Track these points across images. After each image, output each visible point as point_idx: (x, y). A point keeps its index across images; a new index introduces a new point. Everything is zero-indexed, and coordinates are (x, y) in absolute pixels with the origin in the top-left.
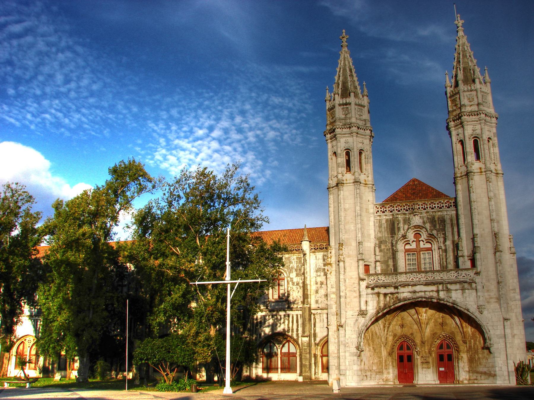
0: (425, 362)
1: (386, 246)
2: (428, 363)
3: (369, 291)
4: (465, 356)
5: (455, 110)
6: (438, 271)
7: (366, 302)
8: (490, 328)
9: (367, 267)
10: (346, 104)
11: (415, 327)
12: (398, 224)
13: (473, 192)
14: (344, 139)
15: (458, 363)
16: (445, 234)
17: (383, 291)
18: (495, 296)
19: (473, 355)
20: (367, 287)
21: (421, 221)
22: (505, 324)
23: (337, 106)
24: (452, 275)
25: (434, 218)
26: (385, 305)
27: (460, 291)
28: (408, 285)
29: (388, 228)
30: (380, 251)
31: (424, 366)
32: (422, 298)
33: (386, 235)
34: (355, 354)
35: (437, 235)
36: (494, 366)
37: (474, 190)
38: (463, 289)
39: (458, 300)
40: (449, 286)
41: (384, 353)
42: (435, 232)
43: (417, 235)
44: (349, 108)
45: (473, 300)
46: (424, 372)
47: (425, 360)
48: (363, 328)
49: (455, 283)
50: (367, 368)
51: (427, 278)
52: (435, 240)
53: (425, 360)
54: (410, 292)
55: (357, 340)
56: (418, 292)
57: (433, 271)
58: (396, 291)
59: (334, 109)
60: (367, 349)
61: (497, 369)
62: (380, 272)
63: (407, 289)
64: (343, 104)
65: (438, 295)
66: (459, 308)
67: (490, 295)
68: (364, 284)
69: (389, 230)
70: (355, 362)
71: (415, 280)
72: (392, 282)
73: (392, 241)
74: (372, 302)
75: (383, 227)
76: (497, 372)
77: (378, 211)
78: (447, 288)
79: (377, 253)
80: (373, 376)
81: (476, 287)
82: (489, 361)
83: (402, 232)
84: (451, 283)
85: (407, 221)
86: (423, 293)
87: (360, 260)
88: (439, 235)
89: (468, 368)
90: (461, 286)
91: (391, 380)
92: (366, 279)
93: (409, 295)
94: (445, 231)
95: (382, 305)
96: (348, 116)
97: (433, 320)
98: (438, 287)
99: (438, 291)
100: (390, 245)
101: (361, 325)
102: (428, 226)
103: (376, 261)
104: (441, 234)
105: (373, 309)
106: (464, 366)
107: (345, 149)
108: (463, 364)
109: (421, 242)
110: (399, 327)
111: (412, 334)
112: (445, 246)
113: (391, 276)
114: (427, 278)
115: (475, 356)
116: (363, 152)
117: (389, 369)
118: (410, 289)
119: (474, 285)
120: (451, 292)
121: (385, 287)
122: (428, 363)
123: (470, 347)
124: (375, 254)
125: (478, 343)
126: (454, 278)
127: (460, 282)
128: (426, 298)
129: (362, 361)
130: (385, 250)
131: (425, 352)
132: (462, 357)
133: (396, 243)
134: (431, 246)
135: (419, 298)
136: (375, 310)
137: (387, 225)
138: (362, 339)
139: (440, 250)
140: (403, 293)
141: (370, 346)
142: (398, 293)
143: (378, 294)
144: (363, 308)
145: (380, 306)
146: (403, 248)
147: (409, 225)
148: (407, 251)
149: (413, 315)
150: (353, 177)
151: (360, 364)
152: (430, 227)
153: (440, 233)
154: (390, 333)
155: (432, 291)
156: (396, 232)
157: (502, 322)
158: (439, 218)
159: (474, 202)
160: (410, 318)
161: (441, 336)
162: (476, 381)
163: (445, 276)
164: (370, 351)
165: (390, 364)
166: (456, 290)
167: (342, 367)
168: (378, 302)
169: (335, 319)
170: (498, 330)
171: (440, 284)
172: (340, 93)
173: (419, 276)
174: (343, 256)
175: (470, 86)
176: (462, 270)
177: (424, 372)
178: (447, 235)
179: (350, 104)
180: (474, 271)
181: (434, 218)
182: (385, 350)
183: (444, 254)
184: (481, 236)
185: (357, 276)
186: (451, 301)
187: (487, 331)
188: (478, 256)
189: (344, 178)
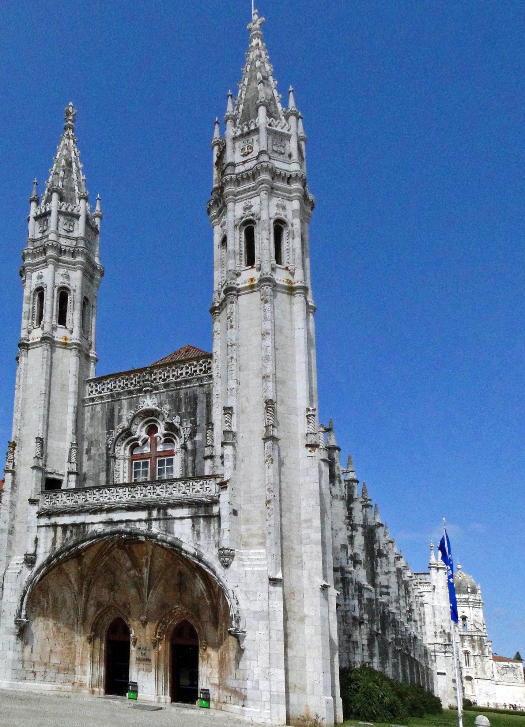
0: (144, 660)
1: (98, 450)
27: (190, 521)
29: (104, 418)
31: (141, 666)
34: (12, 631)
35: (181, 424)
40: (171, 512)
42: (176, 421)
43: (152, 430)
47: (144, 654)
50: (38, 660)
53: (144, 654)
65: (150, 528)
70: (12, 645)
78: (166, 514)
80: (51, 674)
83: (125, 424)
91: (88, 686)
98: (150, 514)
99: (149, 521)
100: (104, 448)
113: (76, 495)
117: (86, 665)
118: (103, 517)
120: (173, 523)
122: (149, 660)
130: (97, 457)
131: (146, 639)
146: (127, 452)
151: (20, 650)
155: (140, 520)
156: (116, 424)
166: (182, 518)
178: (198, 424)
186: (169, 539)
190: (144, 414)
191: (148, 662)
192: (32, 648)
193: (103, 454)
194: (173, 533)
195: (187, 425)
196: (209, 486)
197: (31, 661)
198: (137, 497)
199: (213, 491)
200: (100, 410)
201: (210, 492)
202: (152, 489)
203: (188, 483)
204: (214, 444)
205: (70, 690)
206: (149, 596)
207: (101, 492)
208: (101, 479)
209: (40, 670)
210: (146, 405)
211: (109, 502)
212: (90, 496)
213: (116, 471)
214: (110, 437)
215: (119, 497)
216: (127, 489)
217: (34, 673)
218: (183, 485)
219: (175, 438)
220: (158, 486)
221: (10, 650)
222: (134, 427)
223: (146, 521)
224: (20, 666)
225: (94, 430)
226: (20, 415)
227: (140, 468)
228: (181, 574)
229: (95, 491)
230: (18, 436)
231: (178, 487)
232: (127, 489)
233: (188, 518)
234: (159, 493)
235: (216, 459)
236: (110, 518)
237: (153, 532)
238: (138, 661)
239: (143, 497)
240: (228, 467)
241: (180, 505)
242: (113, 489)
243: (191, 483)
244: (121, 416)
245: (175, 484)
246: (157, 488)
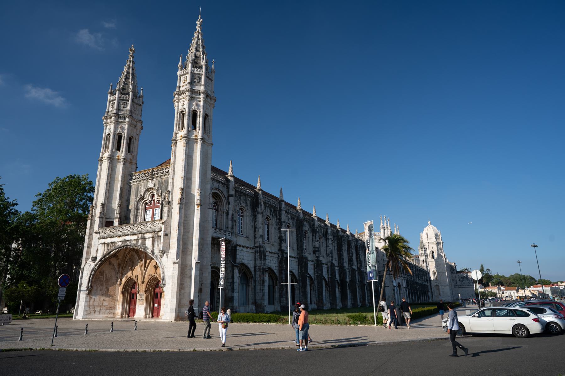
26: (107, 252)
47: (141, 297)
49: (149, 233)
93: (120, 244)
95: (105, 252)
105: (100, 256)
114: (133, 230)
118: (122, 238)
120: (146, 240)
126: (149, 228)
128: (129, 246)
131: (142, 290)
136: (101, 257)
141: (102, 286)
144: (94, 256)
155: (134, 240)
165: (121, 301)
166: (149, 238)
171: (140, 234)
191: (142, 301)
194: (145, 245)
199: (160, 226)
205: (112, 317)
209: (98, 309)
217: (95, 311)
224: (88, 308)
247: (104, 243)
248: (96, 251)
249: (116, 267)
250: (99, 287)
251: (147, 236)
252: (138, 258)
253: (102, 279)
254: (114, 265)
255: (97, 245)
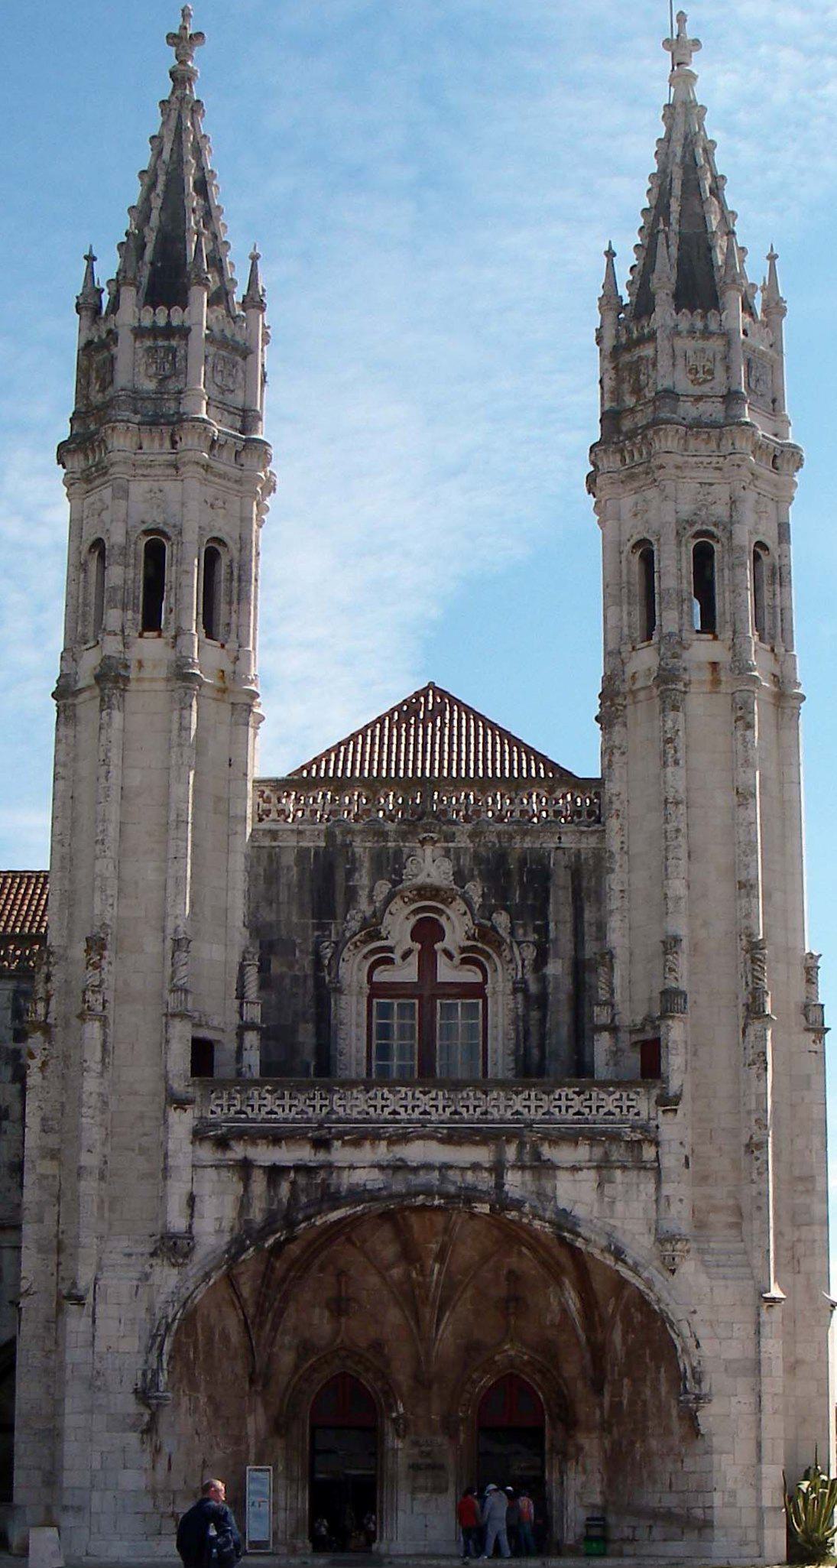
1: (291, 967)
2: (436, 1467)
3: (207, 1153)
4: (591, 1444)
5: (632, 410)
6: (502, 1085)
7: (192, 1200)
8: (702, 1332)
9: (202, 1054)
10: (169, 332)
11: (394, 1316)
12: (349, 874)
13: (676, 763)
14: (145, 485)
15: (562, 1473)
16: (543, 931)
17: (265, 1155)
18: (731, 1202)
19: (625, 1443)
20: (198, 1135)
21: (447, 866)
22: (765, 1316)
23: (125, 338)
24: (563, 1103)
25: (502, 856)
27: (592, 1175)
28: (375, 1137)
30: (264, 984)
31: (421, 1482)
32: (429, 1192)
33: (293, 918)
36: (704, 1489)
37: (679, 754)
38: (603, 1166)
39: (580, 1211)
41: (256, 1423)
42: (502, 920)
43: (427, 932)
44: (180, 353)
45: (641, 1215)
46: (418, 1508)
48: (171, 1312)
51: (456, 1112)
52: (500, 956)
53: (428, 1454)
54: (381, 1167)
55: (141, 1361)
56: (415, 1170)
57: (484, 1085)
58: (322, 1156)
59: (115, 350)
60: (185, 1401)
61: (717, 1499)
62: (256, 1073)
63: (367, 1154)
64: (154, 332)
65: (500, 1185)
66: (579, 1243)
67: (711, 1197)
68: (182, 1123)
69: (307, 898)
71: (403, 1116)
72: (309, 1121)
73: (318, 943)
74: (214, 1200)
75: (283, 880)
76: (716, 1512)
77: (268, 812)
78: (537, 1155)
79: (252, 991)
81: (657, 1159)
82: (689, 1464)
84: (555, 1141)
85: (390, 865)
86: (436, 1173)
87: (174, 1015)
88: (521, 931)
89: (602, 1493)
90: (598, 1152)
92: (198, 1099)
94: (544, 916)
95: (257, 1215)
96: (172, 385)
97: (469, 1293)
100: (307, 962)
101: (162, 1298)
102: (475, 890)
103: (243, 1028)
104: (530, 929)
105: (219, 1231)
106: (584, 1486)
107: (144, 527)
108: (584, 1478)
109: (441, 960)
110: (327, 1314)
111: (377, 1346)
112: (543, 980)
113: (302, 1097)
114: (456, 1112)
115: (632, 1443)
116: (220, 549)
118: (382, 1152)
119: (649, 1152)
120: (555, 1177)
121: (276, 1138)
122: (436, 1467)
123: (616, 1407)
124: (241, 996)
125: (648, 1392)
126: (570, 1116)
127: (593, 1137)
129: (157, 1451)
130: (287, 981)
132: (580, 1449)
133: (337, 955)
134: (479, 979)
135: (417, 1194)
136: (227, 1238)
137: (302, 872)
138: (165, 1358)
139: (520, 996)
140: (352, 1167)
142: (329, 1167)
143: (245, 1167)
144: (177, 1223)
145: (248, 1222)
147: (395, 883)
148: (377, 990)
149: (388, 1268)
150: (170, 654)
151: (148, 1466)
152: (483, 895)
153: (524, 926)
154: (287, 1339)
155: (476, 1167)
156: (339, 910)
157: (751, 1311)
158: (523, 862)
159: (677, 803)
160: (373, 1280)
161: (497, 1358)
162: (628, 1549)
163: (527, 1105)
164: (194, 1410)
166: (575, 1169)
167: (71, 1478)
168: (244, 1204)
169: (52, 1268)
170: (734, 1343)
172: (145, 281)
173: (425, 1101)
174: (100, 998)
175: (704, 317)
176: (603, 1085)
177: (418, 1508)
178: (552, 935)
179: (184, 332)
180: (655, 1092)
181: (502, 856)
182: (260, 1410)
183: (535, 1014)
184: (695, 948)
185: (161, 1086)
187: (691, 1343)
188: (676, 1032)
189: (132, 656)
190: (415, 892)
192: (170, 1460)
193: (306, 976)
195: (525, 934)
196: (633, 1103)
197: (169, 1491)
198: (465, 1115)
199: (644, 1115)
200: (292, 863)
201: (637, 1117)
202: (502, 1099)
203: (587, 1093)
204: (617, 997)
206: (442, 1327)
207: (371, 1094)
208: (301, 1039)
210: (424, 874)
211: (397, 1122)
212: (342, 1102)
213: (341, 1023)
214: (324, 936)
215: (421, 1110)
216: (440, 1093)
218: (575, 1096)
219: (489, 957)
220: (517, 1093)
221: (125, 1468)
222: (387, 918)
223: (489, 1170)
225: (278, 912)
226: (111, 867)
227: (393, 1019)
228: (513, 1277)
229: (355, 1091)
230: (107, 922)
231: (563, 1098)
232: (440, 1093)
233: (588, 1168)
234: (521, 1109)
235: (620, 1035)
236: (398, 1156)
237: (510, 1195)
238: (411, 1470)
239: (482, 1114)
240: (675, 1068)
241: (572, 1138)
242: (403, 1089)
243: (594, 1095)
244: (355, 887)
245: (558, 1091)
246: (514, 1097)
247: (245, 1167)
248: (184, 1199)
249: (246, 1291)
250: (182, 1393)
251: (562, 1155)
252: (389, 1252)
253: (192, 1356)
254: (243, 1279)
255: (189, 1170)
